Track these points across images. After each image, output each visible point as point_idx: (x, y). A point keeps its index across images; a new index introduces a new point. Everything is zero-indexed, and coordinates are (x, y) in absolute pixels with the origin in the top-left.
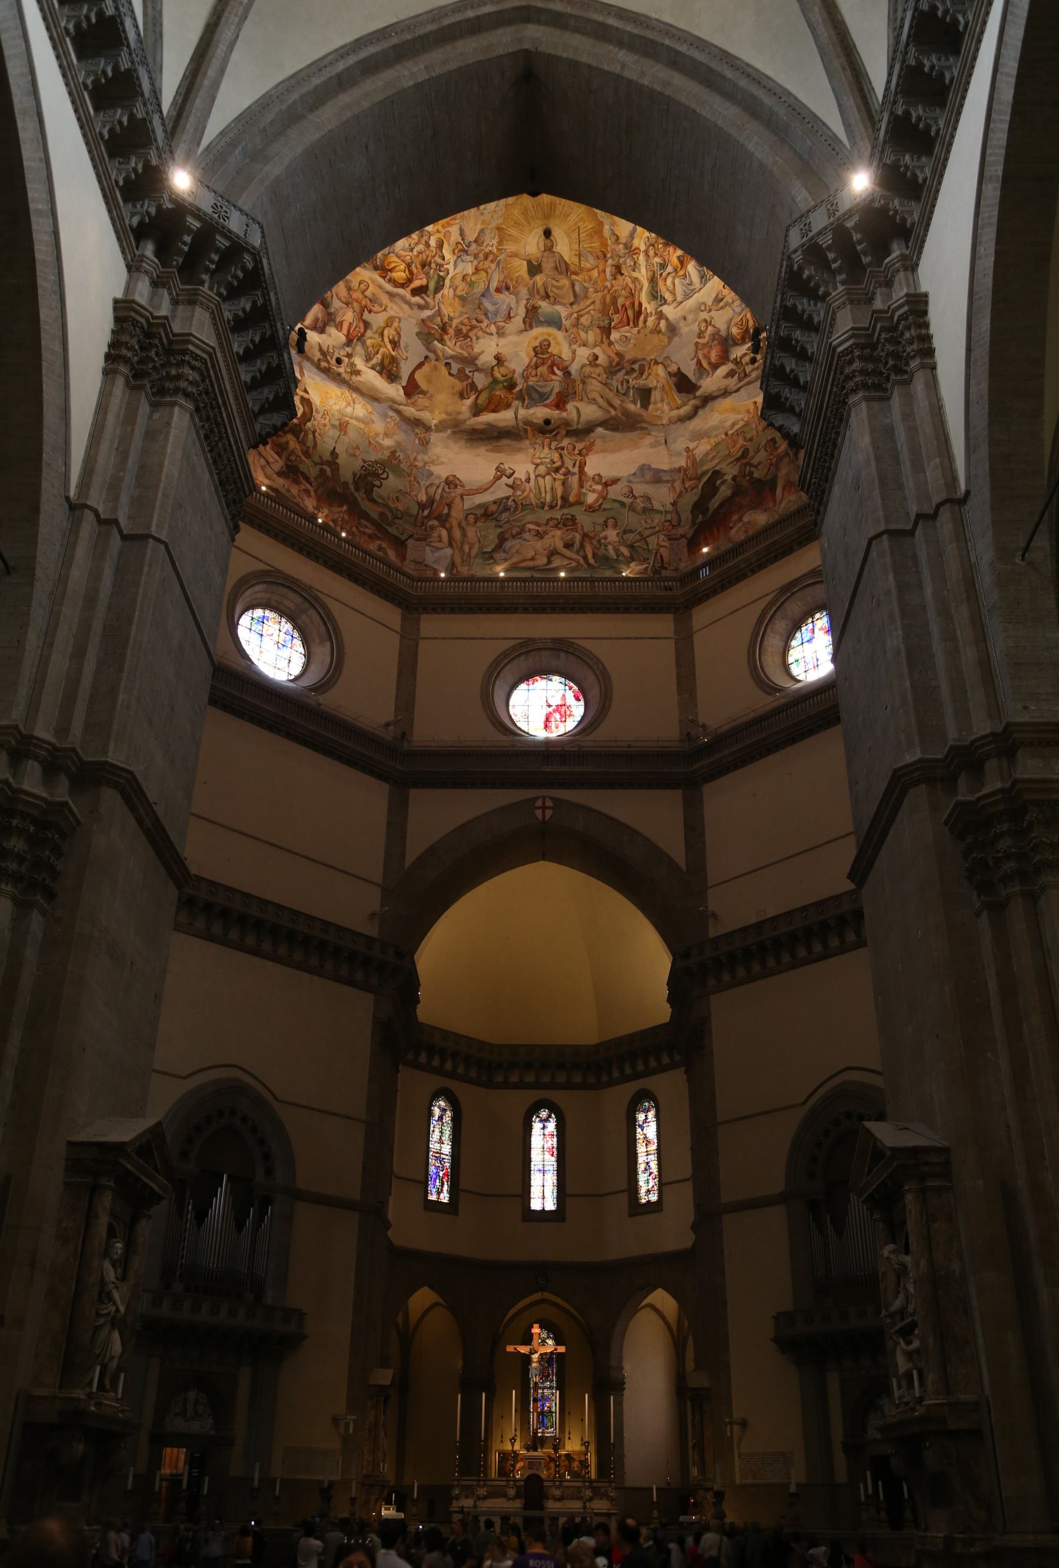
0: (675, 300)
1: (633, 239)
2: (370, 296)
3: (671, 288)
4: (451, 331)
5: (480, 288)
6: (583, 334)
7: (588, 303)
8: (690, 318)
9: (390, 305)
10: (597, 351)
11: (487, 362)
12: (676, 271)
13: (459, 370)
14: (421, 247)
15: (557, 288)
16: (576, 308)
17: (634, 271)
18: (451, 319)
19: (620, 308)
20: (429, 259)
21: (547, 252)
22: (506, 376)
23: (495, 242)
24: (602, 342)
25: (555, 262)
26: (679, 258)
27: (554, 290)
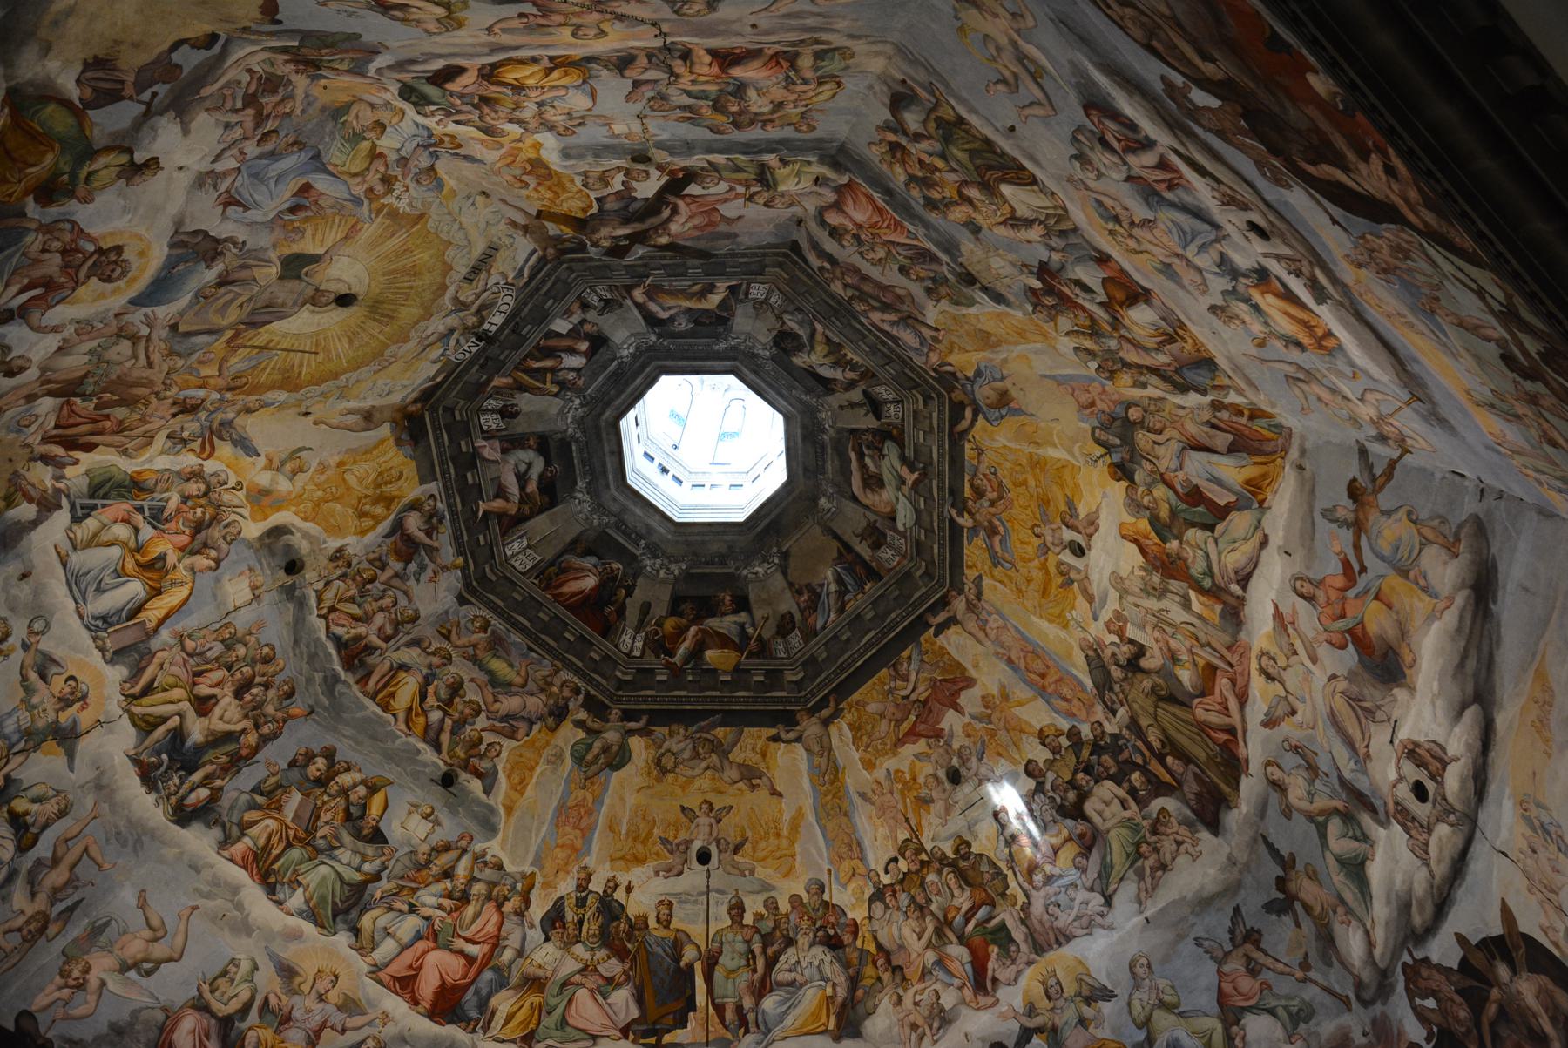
0: (75, 548)
1: (235, 443)
2: (552, 30)
3: (105, 537)
4: (285, 69)
5: (335, 154)
6: (94, 344)
7: (156, 357)
8: (23, 591)
9: (484, 38)
10: (33, 373)
11: (154, 139)
12: (138, 549)
13: (179, 67)
14: (529, 110)
15: (231, 301)
16: (164, 333)
17: (169, 437)
18: (314, 78)
19: (106, 411)
20: (486, 110)
21: (310, 292)
22: (87, 180)
23: (403, 206)
24: (49, 382)
25: (283, 305)
26: (162, 558)
27: (231, 295)
